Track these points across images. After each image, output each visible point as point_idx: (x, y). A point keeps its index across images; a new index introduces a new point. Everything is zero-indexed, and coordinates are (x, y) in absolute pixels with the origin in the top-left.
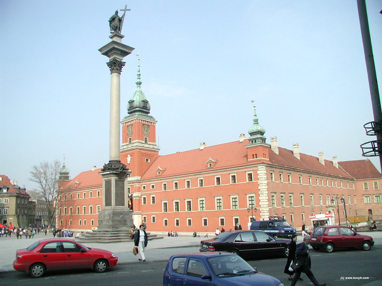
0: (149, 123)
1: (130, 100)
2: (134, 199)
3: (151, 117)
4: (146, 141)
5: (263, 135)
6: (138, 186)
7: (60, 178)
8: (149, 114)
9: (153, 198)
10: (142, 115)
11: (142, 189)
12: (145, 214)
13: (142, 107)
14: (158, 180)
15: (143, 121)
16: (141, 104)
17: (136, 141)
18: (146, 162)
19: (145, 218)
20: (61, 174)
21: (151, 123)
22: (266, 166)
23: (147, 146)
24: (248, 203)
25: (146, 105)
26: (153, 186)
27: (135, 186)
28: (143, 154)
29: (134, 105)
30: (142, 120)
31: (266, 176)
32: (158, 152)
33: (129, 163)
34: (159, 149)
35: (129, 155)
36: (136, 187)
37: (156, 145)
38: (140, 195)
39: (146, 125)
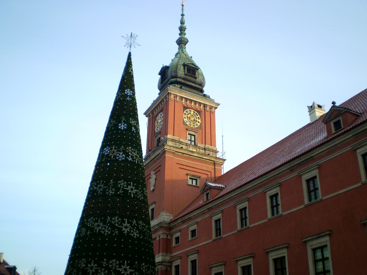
3: (205, 95)
6: (165, 237)
9: (194, 262)
10: (181, 88)
11: (174, 244)
13: (183, 76)
14: (204, 213)
15: (184, 100)
21: (205, 106)
25: (195, 74)
26: (193, 232)
27: (158, 239)
29: (167, 74)
33: (152, 188)
34: (224, 158)
35: (153, 173)
36: (159, 240)
37: (216, 152)
38: (168, 258)
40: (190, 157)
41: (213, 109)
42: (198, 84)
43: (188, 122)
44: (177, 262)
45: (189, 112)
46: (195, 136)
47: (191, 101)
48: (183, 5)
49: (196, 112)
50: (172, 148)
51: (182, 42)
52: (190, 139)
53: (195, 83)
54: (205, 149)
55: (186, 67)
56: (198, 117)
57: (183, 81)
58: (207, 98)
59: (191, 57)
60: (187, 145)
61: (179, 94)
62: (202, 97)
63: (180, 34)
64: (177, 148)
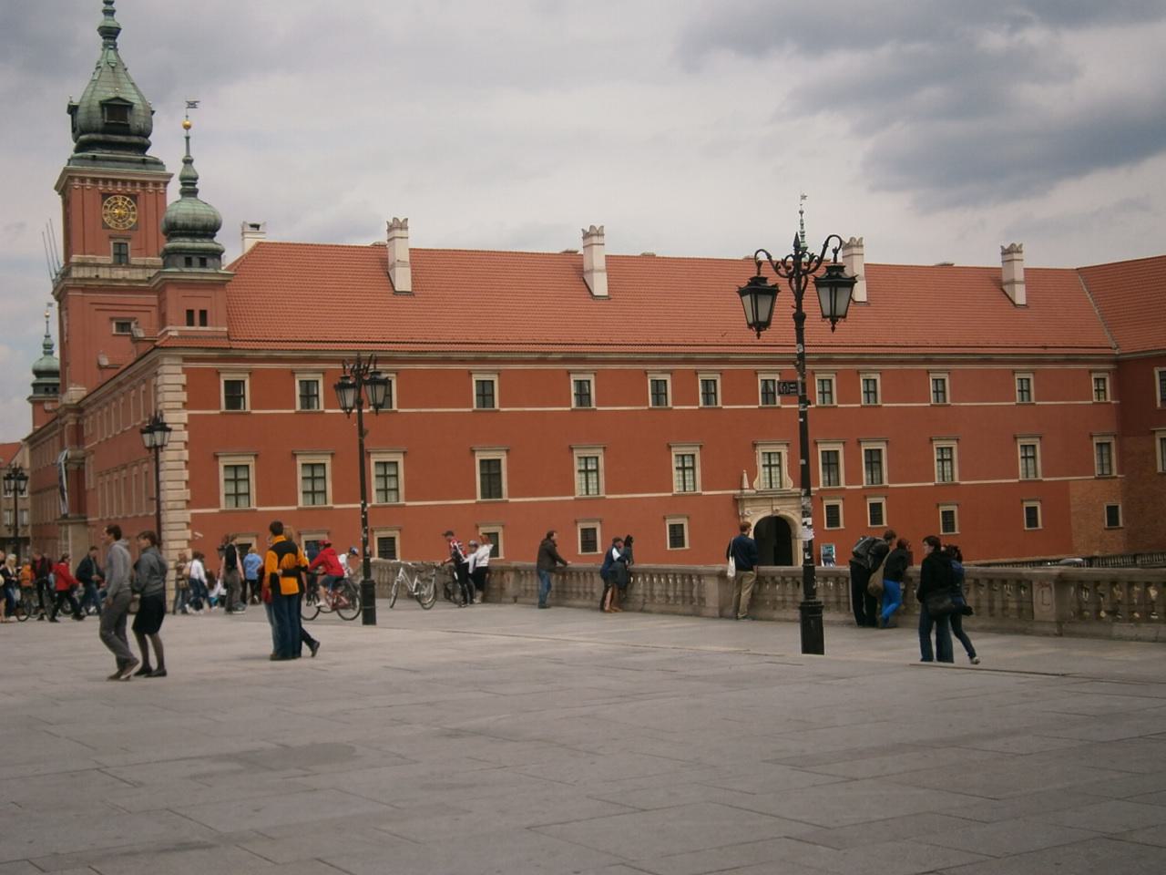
1: (69, 106)
3: (144, 162)
4: (121, 258)
5: (215, 239)
7: (35, 392)
8: (148, 153)
13: (100, 126)
16: (100, 115)
18: (114, 332)
20: (38, 373)
21: (144, 184)
22: (186, 359)
23: (120, 273)
24: (223, 491)
25: (126, 119)
28: (98, 307)
30: (95, 180)
31: (184, 396)
38: (80, 453)
39: (120, 194)
40: (111, 287)
41: (162, 185)
42: (135, 135)
43: (114, 222)
45: (114, 202)
46: (126, 244)
47: (115, 181)
49: (128, 199)
50: (78, 282)
51: (110, 34)
52: (117, 251)
54: (144, 267)
55: (105, 109)
56: (133, 208)
57: (100, 137)
58: (150, 166)
59: (126, 69)
60: (110, 266)
61: (88, 175)
62: (139, 165)
64: (90, 279)
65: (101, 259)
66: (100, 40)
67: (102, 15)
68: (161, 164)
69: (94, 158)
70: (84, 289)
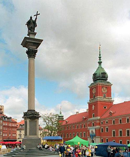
0: (107, 86)
2: (96, 129)
3: (108, 82)
8: (107, 81)
9: (107, 128)
10: (101, 81)
11: (101, 124)
12: (102, 138)
13: (101, 77)
17: (98, 97)
19: (102, 140)
21: (108, 86)
30: (101, 85)
32: (112, 102)
33: (93, 109)
35: (93, 105)
36: (97, 123)
44: (102, 128)
47: (104, 85)
48: (100, 48)
53: (105, 78)
54: (108, 98)
60: (103, 98)
63: (99, 60)
65: (102, 97)
66: (98, 64)
67: (99, 60)
68: (109, 82)
69: (101, 81)
70: (100, 102)
